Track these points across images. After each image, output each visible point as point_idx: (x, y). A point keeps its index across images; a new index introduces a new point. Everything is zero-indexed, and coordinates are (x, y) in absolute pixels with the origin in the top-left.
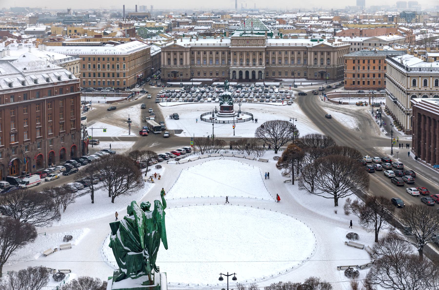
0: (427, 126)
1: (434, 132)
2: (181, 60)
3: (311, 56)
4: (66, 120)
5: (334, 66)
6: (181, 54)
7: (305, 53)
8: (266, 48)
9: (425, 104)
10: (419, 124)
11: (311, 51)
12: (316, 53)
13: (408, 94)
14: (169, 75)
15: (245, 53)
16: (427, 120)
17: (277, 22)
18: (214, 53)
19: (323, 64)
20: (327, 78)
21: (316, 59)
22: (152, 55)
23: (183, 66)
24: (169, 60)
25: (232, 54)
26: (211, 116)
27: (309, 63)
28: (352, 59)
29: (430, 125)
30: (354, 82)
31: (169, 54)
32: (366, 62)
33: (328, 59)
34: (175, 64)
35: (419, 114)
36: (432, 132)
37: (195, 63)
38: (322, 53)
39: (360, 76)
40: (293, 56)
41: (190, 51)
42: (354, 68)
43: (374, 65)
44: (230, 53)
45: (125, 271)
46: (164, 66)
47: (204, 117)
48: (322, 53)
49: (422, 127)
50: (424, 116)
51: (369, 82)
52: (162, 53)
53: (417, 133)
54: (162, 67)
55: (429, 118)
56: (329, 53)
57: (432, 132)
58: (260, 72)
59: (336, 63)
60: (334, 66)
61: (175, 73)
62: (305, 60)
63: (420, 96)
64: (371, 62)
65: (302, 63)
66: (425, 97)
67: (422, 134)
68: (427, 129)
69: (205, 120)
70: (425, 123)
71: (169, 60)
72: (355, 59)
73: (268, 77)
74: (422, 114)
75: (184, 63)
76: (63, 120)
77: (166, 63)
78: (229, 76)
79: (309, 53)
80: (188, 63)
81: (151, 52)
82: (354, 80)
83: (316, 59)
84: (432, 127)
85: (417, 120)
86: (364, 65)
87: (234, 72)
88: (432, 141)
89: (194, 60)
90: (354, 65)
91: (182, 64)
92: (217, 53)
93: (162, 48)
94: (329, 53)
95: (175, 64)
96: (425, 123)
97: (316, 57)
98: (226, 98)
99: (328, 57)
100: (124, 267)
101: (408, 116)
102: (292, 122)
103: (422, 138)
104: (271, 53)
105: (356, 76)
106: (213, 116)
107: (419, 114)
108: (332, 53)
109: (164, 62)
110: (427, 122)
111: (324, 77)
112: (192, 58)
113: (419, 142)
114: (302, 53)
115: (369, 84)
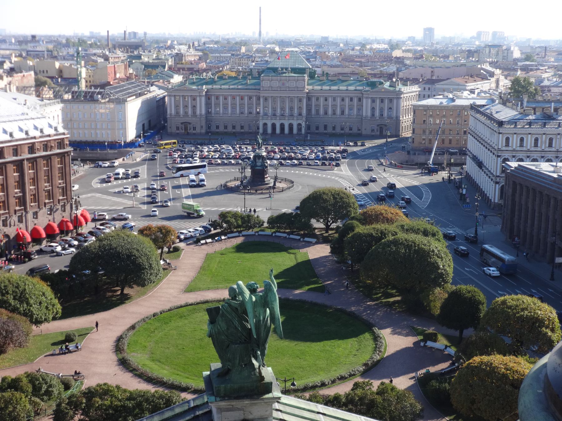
0: (524, 198)
2: (194, 107)
3: (367, 104)
4: (52, 186)
6: (194, 99)
7: (360, 100)
8: (307, 93)
10: (513, 195)
11: (367, 98)
12: (373, 101)
13: (498, 156)
14: (178, 128)
15: (279, 99)
16: (525, 190)
18: (238, 98)
19: (382, 115)
20: (389, 134)
21: (373, 109)
23: (196, 116)
24: (177, 106)
25: (261, 100)
27: (364, 114)
28: (422, 108)
30: (424, 139)
33: (391, 108)
35: (514, 183)
36: (530, 205)
37: (213, 112)
38: (382, 101)
40: (342, 103)
41: (206, 95)
44: (258, 98)
46: (171, 115)
48: (382, 101)
49: (517, 199)
50: (521, 185)
53: (510, 207)
54: (168, 116)
57: (530, 205)
58: (299, 125)
62: (360, 109)
63: (514, 159)
65: (355, 113)
66: (521, 160)
67: (517, 208)
68: (523, 203)
72: (426, 108)
73: (309, 131)
75: (198, 112)
77: (173, 112)
78: (258, 128)
79: (364, 100)
80: (203, 112)
82: (424, 137)
85: (511, 191)
87: (265, 124)
88: (529, 217)
89: (211, 108)
91: (194, 113)
92: (242, 98)
94: (391, 100)
98: (259, 159)
99: (390, 106)
101: (497, 185)
103: (516, 213)
104: (314, 100)
106: (242, 182)
107: (514, 183)
108: (395, 101)
109: (171, 110)
110: (524, 193)
111: (384, 133)
114: (355, 100)
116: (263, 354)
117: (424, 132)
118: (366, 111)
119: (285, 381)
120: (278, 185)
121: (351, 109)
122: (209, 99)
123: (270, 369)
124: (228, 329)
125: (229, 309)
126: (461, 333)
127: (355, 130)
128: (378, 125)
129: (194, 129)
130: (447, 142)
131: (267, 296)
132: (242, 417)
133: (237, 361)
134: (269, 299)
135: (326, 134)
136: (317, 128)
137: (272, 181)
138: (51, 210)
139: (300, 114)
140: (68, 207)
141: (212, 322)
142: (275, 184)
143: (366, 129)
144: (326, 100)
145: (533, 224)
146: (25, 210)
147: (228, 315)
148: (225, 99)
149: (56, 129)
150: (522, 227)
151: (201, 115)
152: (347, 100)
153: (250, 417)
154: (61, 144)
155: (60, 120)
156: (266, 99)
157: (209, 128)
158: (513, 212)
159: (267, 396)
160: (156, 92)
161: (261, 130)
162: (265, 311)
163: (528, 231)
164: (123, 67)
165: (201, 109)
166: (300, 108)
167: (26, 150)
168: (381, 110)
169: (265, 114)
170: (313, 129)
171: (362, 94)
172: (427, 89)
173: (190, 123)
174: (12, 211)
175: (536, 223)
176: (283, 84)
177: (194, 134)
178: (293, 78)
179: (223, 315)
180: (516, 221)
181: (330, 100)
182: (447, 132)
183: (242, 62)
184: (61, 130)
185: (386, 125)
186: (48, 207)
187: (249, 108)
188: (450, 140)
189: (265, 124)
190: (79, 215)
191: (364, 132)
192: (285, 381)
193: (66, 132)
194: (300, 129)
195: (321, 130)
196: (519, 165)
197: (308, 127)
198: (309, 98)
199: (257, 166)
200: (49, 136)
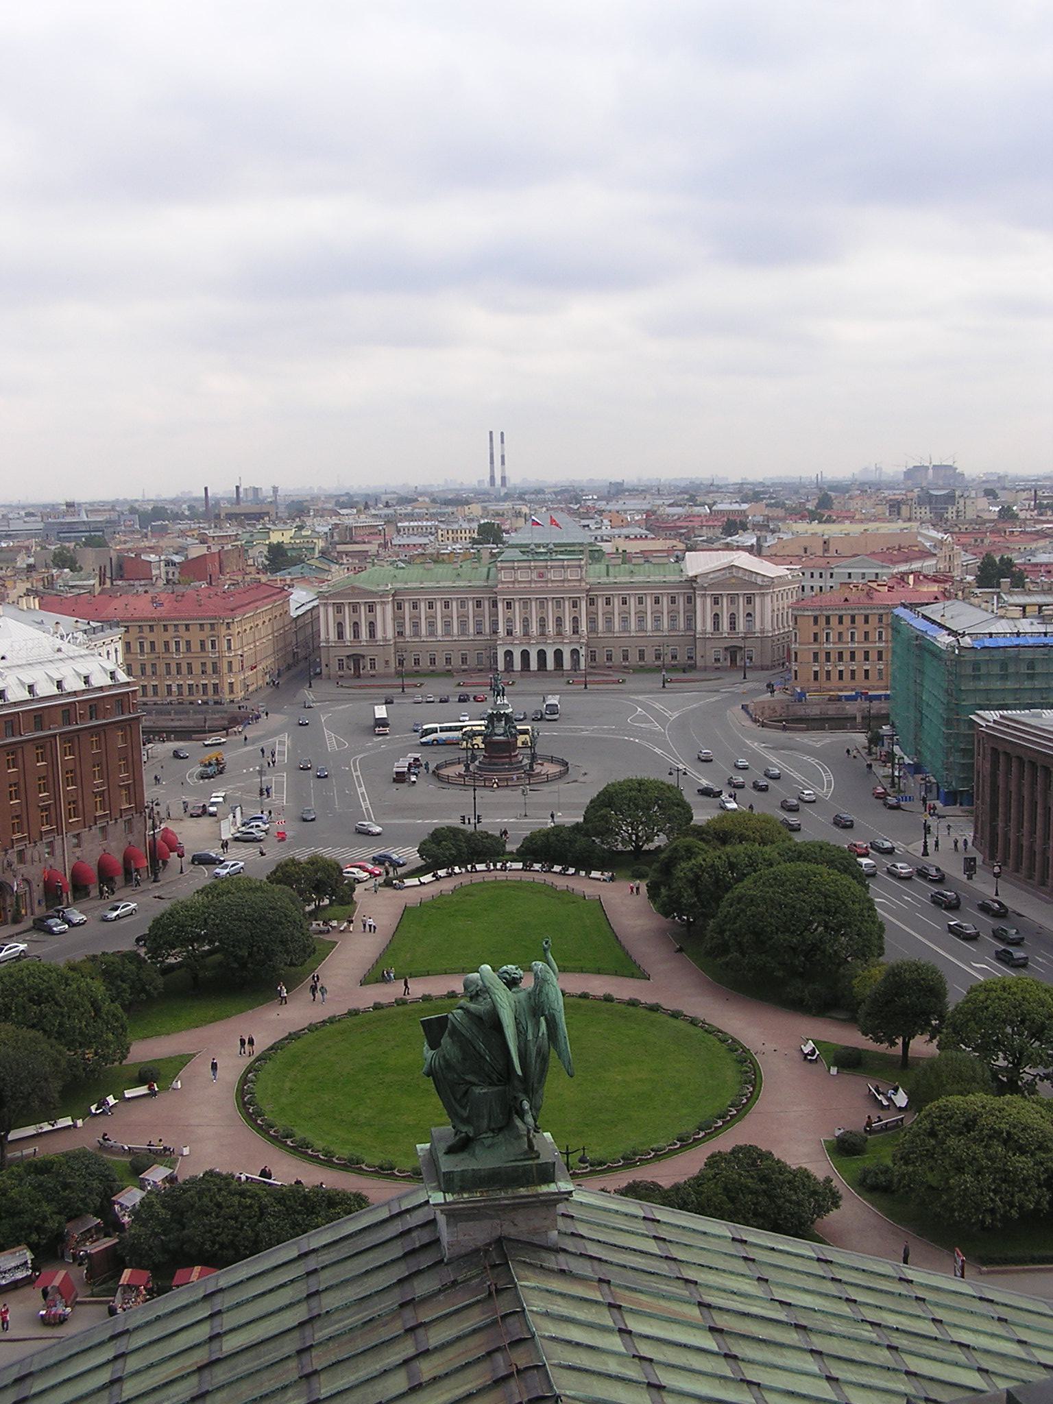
1: (1033, 793)
2: (372, 625)
5: (762, 632)
6: (371, 609)
7: (690, 600)
8: (588, 591)
9: (1008, 726)
10: (994, 774)
14: (341, 667)
17: (606, 522)
21: (716, 615)
22: (294, 614)
24: (340, 625)
25: (500, 605)
26: (461, 769)
27: (699, 628)
29: (1021, 776)
30: (816, 672)
31: (339, 608)
32: (847, 620)
33: (749, 615)
34: (356, 634)
36: (1026, 793)
38: (733, 599)
39: (832, 659)
42: (815, 640)
43: (867, 628)
44: (495, 605)
45: (467, 1130)
46: (327, 641)
47: (444, 772)
48: (733, 599)
51: (853, 672)
52: (322, 609)
55: (1020, 758)
56: (749, 601)
57: (1026, 793)
58: (575, 652)
59: (768, 627)
60: (762, 632)
61: (356, 659)
62: (690, 620)
64: (860, 620)
67: (1001, 800)
68: (1013, 788)
69: (447, 781)
70: (1008, 772)
71: (340, 625)
72: (818, 613)
74: (1000, 749)
76: (102, 784)
77: (333, 636)
78: (496, 662)
79: (698, 600)
80: (390, 635)
81: (293, 606)
82: (817, 669)
83: (716, 615)
84: (1026, 781)
85: (988, 766)
86: (841, 628)
87: (509, 654)
89: (402, 625)
90: (816, 629)
91: (372, 633)
93: (320, 595)
94: (749, 601)
95: (356, 634)
96: (1008, 772)
97: (717, 609)
100: (467, 1121)
102: (671, 781)
104: (601, 602)
105: (822, 657)
106: (467, 766)
108: (757, 599)
109: (327, 632)
112: (399, 621)
113: (994, 818)
114: (681, 601)
115: (853, 678)
116: (536, 1108)
117: (816, 655)
118: (704, 624)
119: (567, 1154)
120: (537, 768)
121: (673, 619)
122: (400, 608)
123: (547, 1135)
124: (464, 1059)
125: (466, 1021)
126: (906, 1045)
127: (682, 659)
128: (726, 649)
129: (373, 666)
130: (860, 675)
131: (541, 991)
132: (496, 1234)
133: (485, 1122)
134: (544, 998)
135: (625, 667)
136: (609, 658)
137: (526, 761)
138: (103, 829)
139: (575, 632)
140: (138, 824)
141: (434, 1045)
142: (531, 767)
143: (707, 654)
144: (624, 603)
145: (1033, 832)
146: (59, 831)
147: (464, 1031)
148: (431, 607)
149: (113, 675)
150: (1012, 836)
151: (385, 639)
152: (665, 601)
153: (511, 1231)
154: (122, 701)
155: (120, 660)
156: (509, 605)
157: (401, 663)
158: (994, 807)
159: (544, 1189)
160: (300, 598)
161: (501, 666)
162: (538, 1024)
163: (1025, 843)
164: (236, 554)
165: (386, 629)
166: (575, 620)
167: (60, 718)
168: (733, 618)
169: (509, 633)
170: (601, 658)
171: (694, 589)
172: (816, 575)
173: (363, 657)
174: (35, 834)
175: (1039, 826)
176: (541, 575)
177: (373, 676)
178: (560, 563)
179: (455, 1033)
180: (1001, 825)
181: (632, 602)
182: (860, 656)
183: (459, 535)
184: (122, 677)
185: (741, 648)
186: (100, 824)
187: (479, 624)
188: (866, 671)
189: (509, 654)
190: (158, 837)
191: (700, 662)
192: (567, 1154)
193: (131, 679)
194: (575, 662)
195: (618, 658)
196: (1001, 716)
197: (593, 659)
198: (592, 602)
199: (496, 735)
200: (101, 689)
